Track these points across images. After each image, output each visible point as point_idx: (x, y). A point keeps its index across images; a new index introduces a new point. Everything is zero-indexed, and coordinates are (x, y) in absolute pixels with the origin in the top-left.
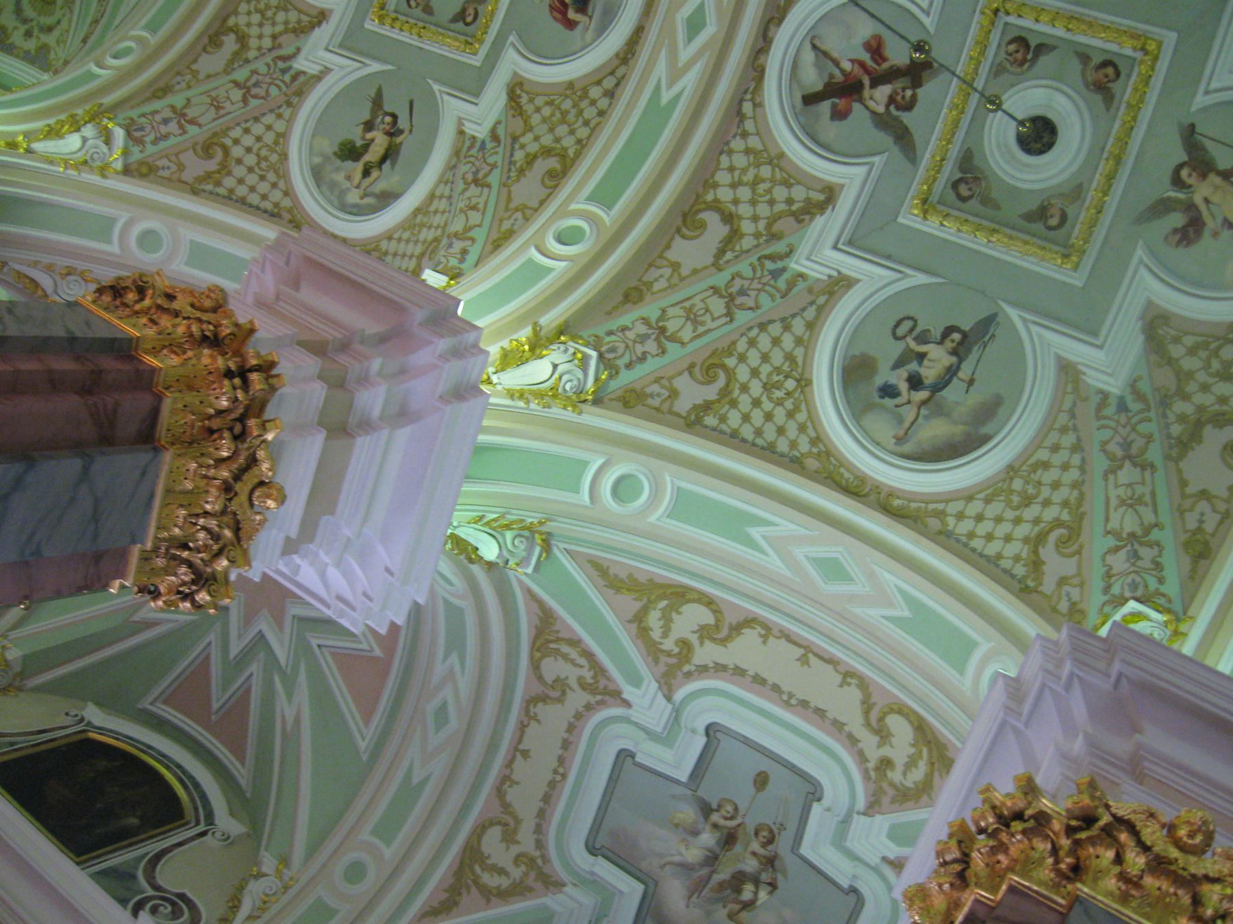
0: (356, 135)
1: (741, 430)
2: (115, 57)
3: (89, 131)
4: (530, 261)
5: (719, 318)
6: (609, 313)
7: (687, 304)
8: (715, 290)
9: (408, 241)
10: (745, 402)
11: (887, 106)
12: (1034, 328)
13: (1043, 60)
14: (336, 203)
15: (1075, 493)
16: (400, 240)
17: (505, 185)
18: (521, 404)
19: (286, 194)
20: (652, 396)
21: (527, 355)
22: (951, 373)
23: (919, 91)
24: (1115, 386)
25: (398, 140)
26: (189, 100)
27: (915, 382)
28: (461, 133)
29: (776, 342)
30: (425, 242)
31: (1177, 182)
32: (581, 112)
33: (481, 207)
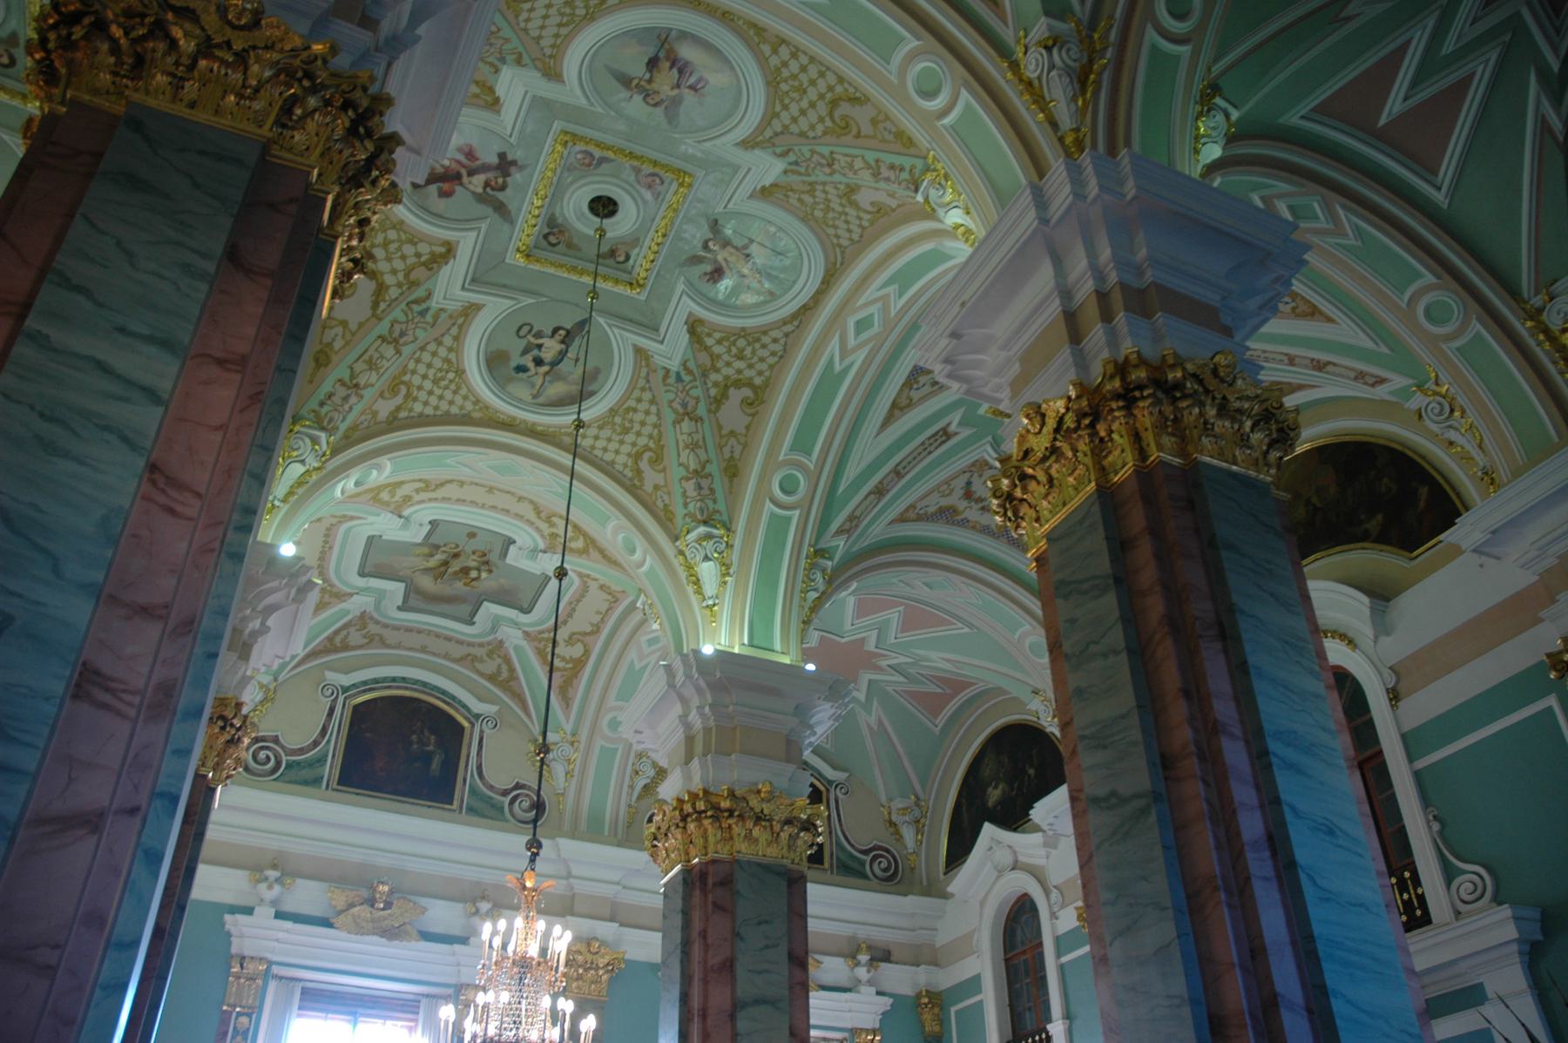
6: (311, 382)
10: (423, 395)
11: (485, 188)
12: (616, 331)
13: (604, 165)
15: (656, 431)
20: (362, 423)
22: (562, 355)
23: (508, 179)
24: (674, 365)
27: (539, 362)
29: (434, 354)
31: (706, 247)
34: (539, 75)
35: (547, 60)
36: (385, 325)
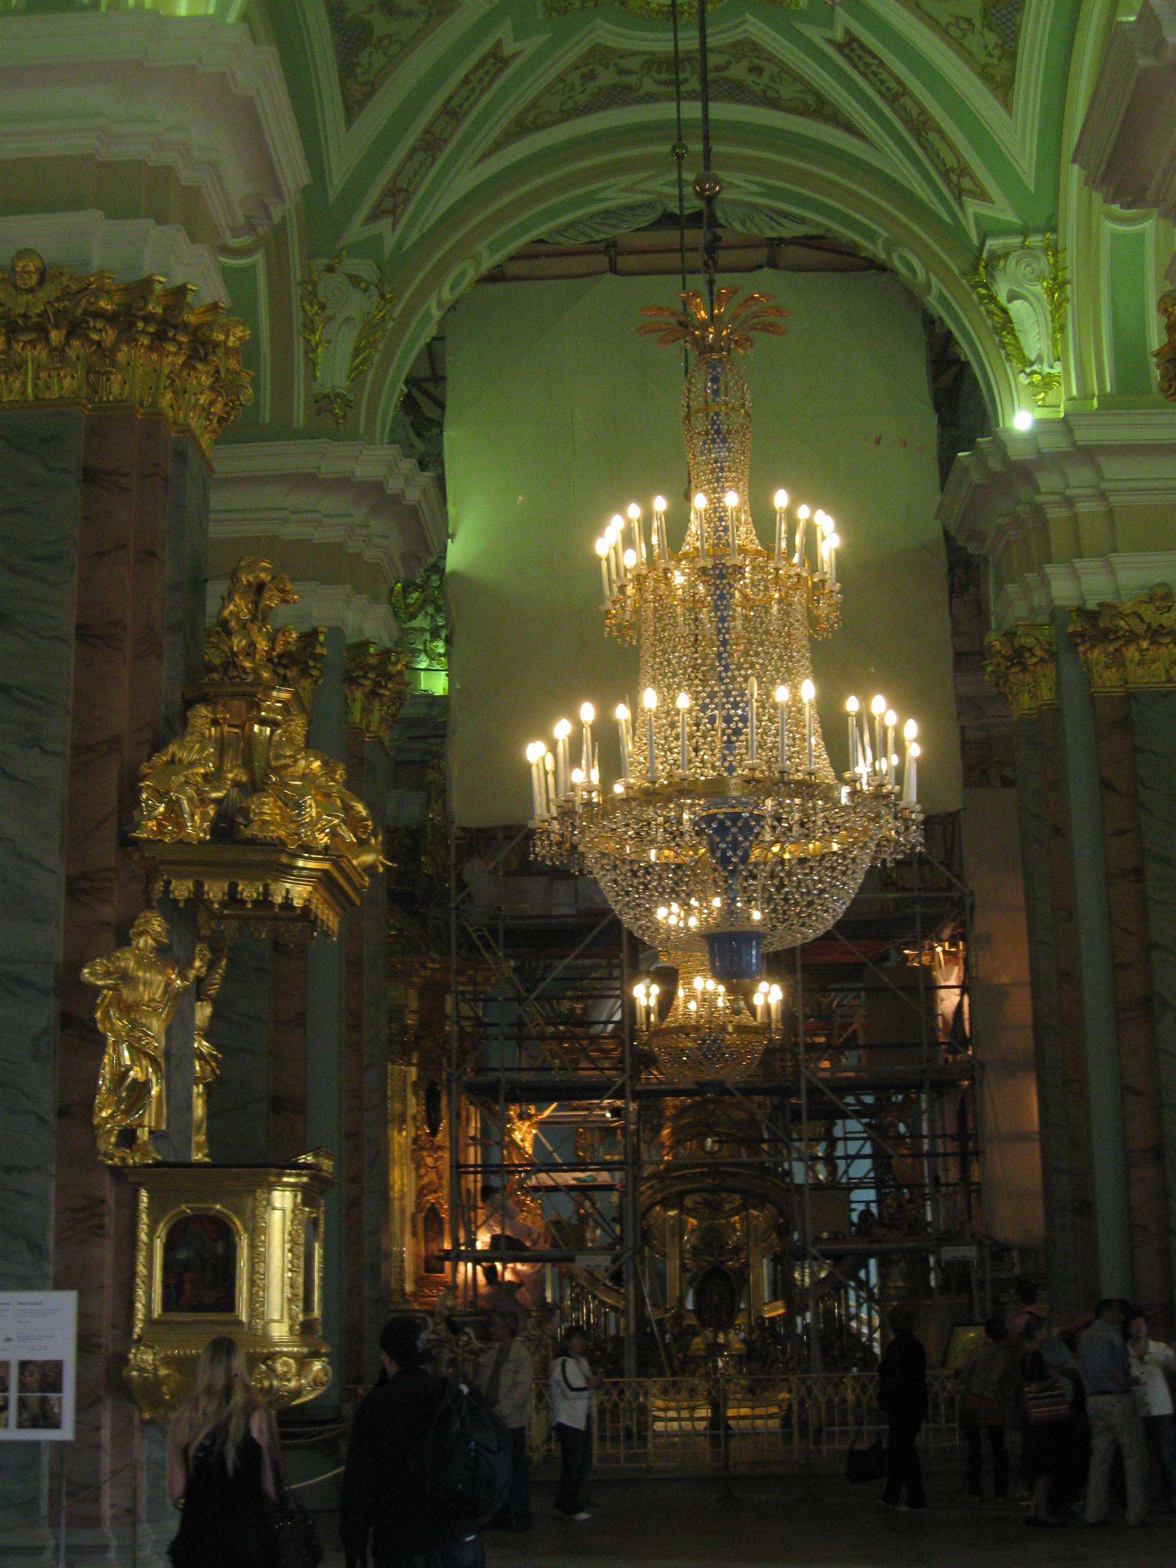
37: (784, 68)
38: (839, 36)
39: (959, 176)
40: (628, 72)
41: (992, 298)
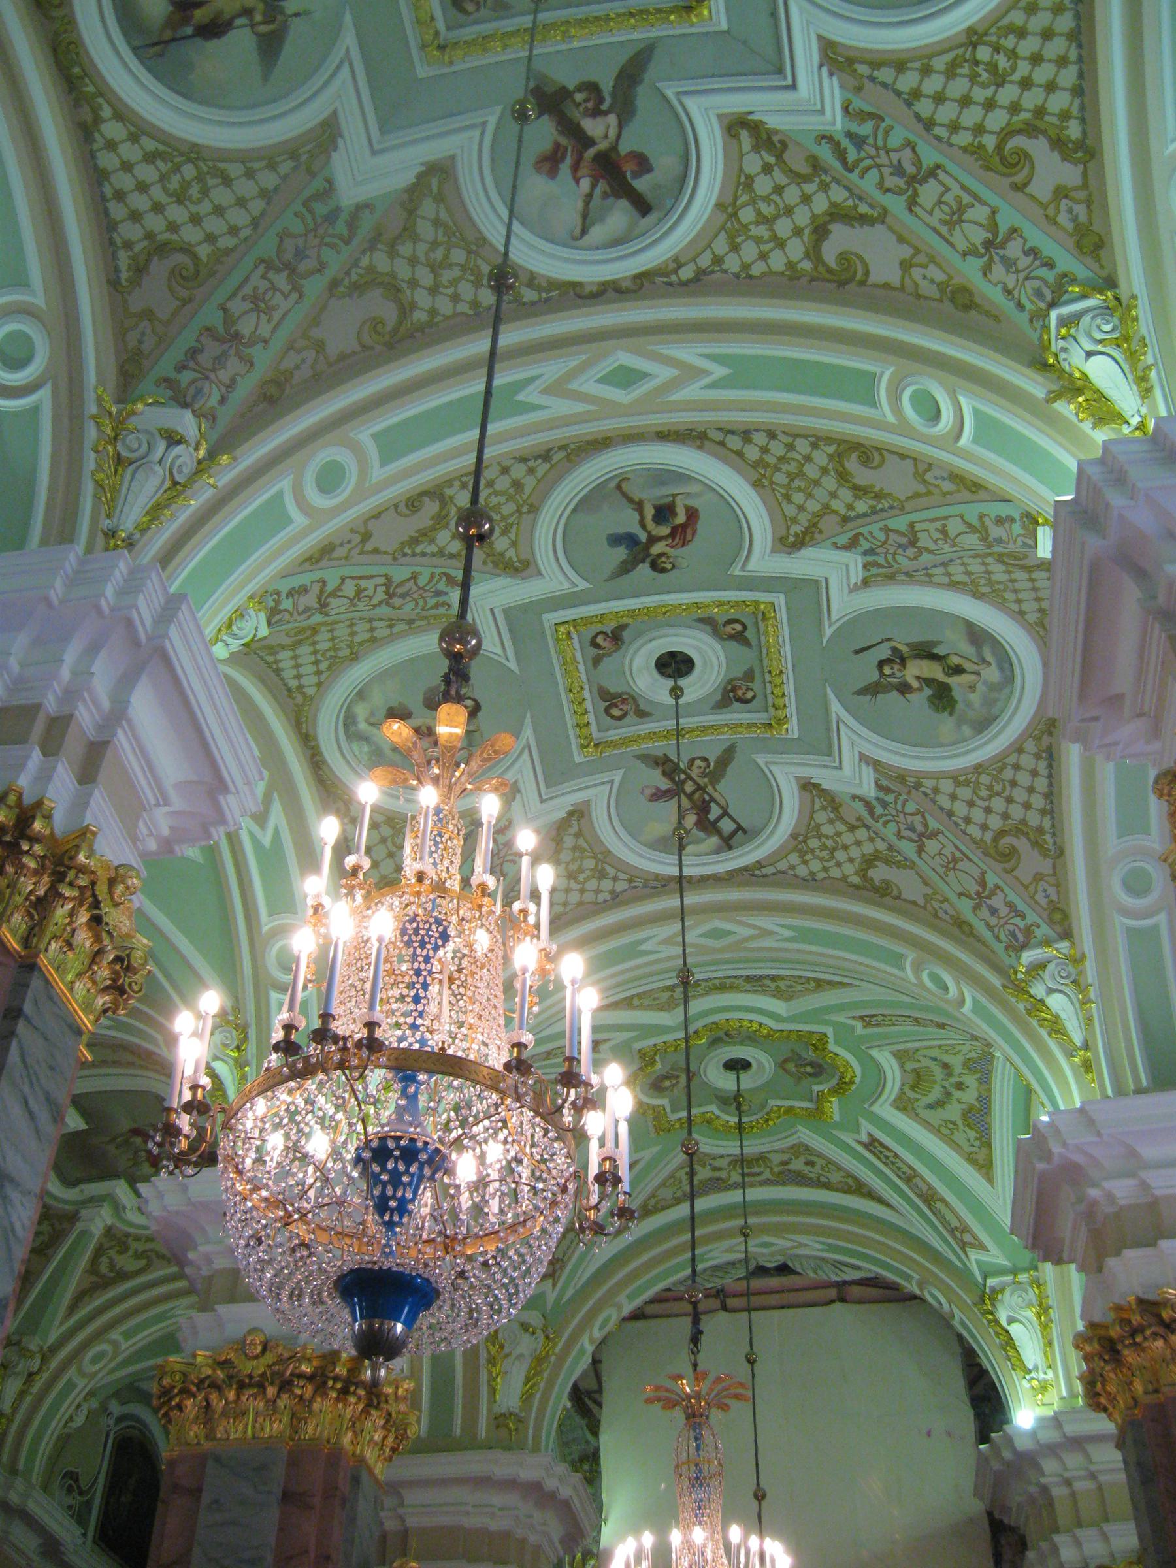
0: (920, 698)
1: (1069, 85)
2: (946, 988)
3: (1038, 990)
4: (976, 440)
5: (944, 185)
6: (997, 319)
7: (944, 230)
8: (912, 204)
9: (1016, 591)
10: (1031, 99)
14: (1007, 691)
16: (1018, 601)
17: (902, 509)
18: (1153, 375)
19: (1020, 751)
20: (1075, 219)
21: (1089, 394)
23: (571, 87)
25: (905, 649)
26: (960, 895)
28: (866, 583)
30: (1009, 572)
32: (781, 459)
33: (938, 525)
34: (335, 156)
35: (304, 158)
36: (888, 200)
37: (830, 1162)
38: (864, 1138)
39: (962, 1233)
40: (719, 1169)
41: (997, 1322)
